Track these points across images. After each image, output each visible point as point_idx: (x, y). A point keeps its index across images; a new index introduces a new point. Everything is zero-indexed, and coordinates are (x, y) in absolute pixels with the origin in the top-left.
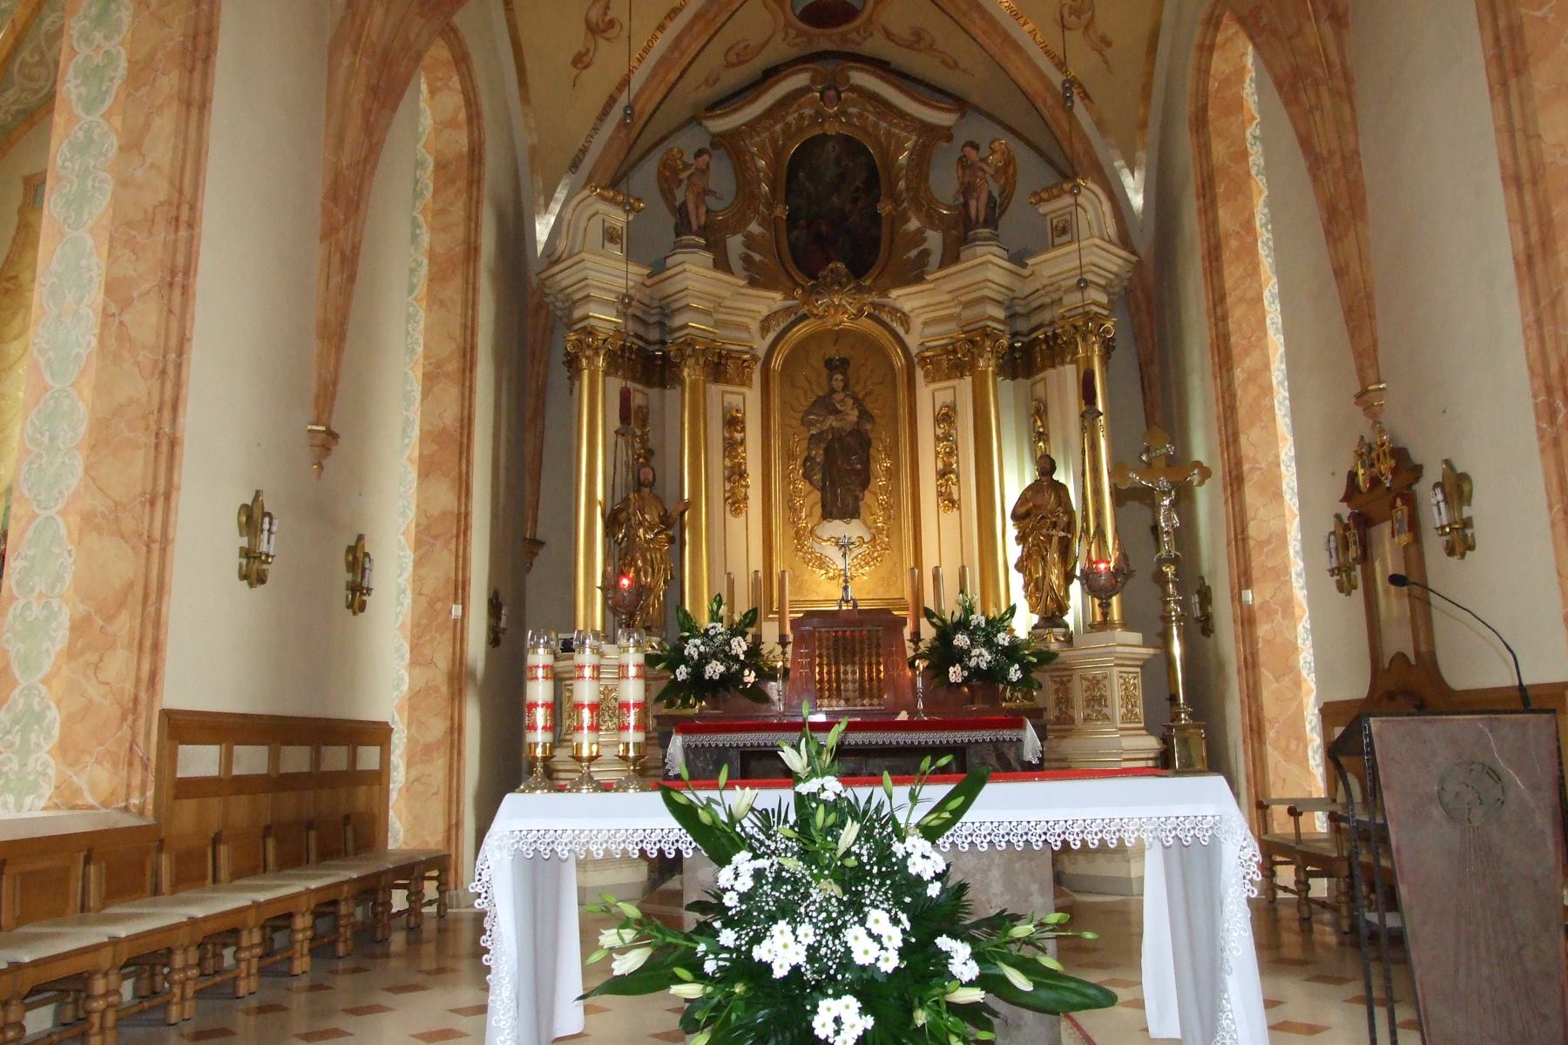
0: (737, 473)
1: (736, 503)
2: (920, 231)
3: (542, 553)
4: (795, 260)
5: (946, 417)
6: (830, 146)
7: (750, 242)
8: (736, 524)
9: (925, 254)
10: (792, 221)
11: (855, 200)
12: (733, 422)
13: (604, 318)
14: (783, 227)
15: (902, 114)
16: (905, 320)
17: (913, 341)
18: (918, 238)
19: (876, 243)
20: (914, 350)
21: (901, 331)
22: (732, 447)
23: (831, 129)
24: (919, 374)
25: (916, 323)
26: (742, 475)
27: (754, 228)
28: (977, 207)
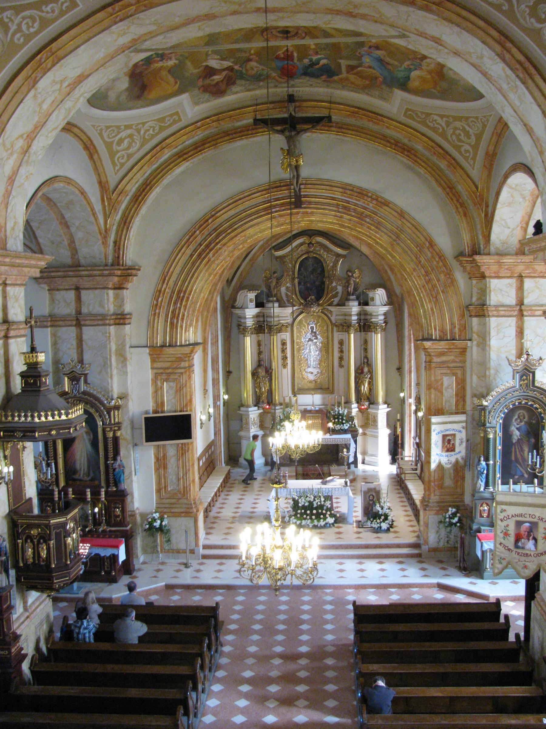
0: (285, 358)
1: (285, 366)
2: (336, 286)
3: (231, 375)
4: (301, 295)
5: (341, 343)
6: (310, 260)
7: (287, 288)
8: (285, 371)
9: (337, 293)
10: (299, 283)
11: (317, 277)
12: (284, 344)
13: (250, 323)
14: (297, 285)
15: (331, 251)
16: (331, 312)
17: (333, 319)
18: (336, 287)
19: (323, 290)
20: (334, 322)
21: (330, 315)
22: (283, 351)
23: (311, 255)
24: (335, 329)
25: (334, 314)
26: (286, 358)
27: (288, 285)
28: (351, 289)
